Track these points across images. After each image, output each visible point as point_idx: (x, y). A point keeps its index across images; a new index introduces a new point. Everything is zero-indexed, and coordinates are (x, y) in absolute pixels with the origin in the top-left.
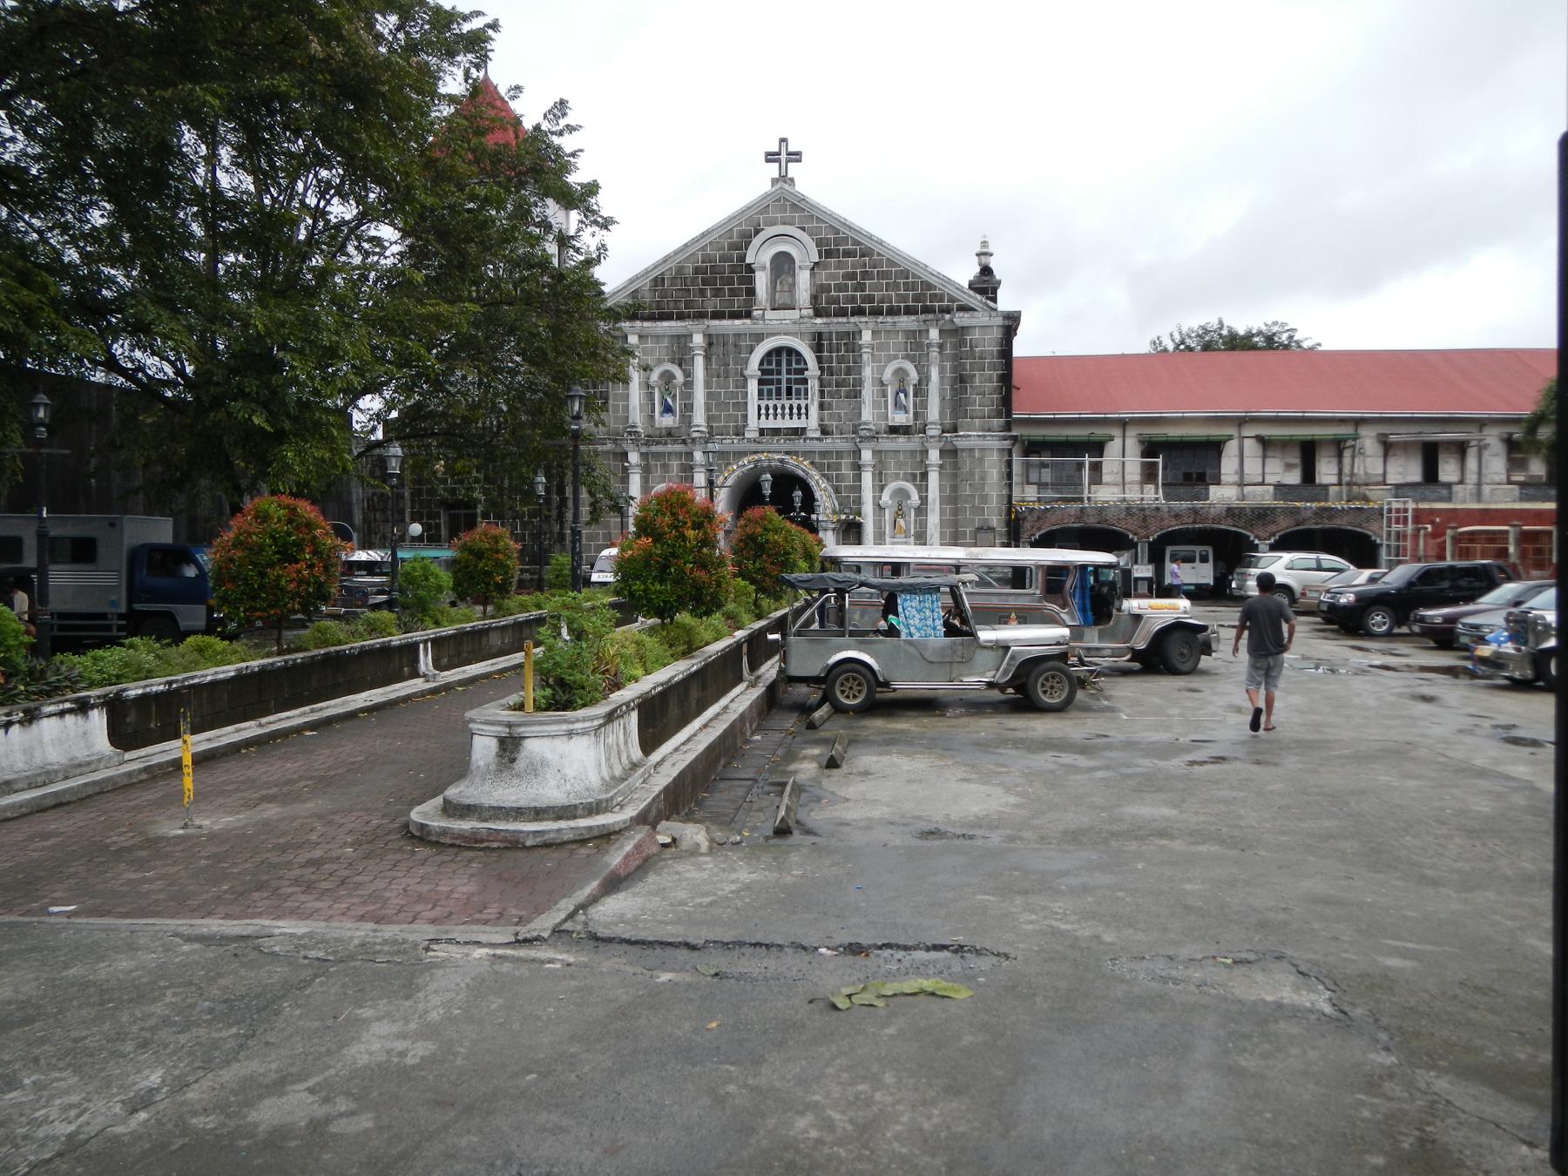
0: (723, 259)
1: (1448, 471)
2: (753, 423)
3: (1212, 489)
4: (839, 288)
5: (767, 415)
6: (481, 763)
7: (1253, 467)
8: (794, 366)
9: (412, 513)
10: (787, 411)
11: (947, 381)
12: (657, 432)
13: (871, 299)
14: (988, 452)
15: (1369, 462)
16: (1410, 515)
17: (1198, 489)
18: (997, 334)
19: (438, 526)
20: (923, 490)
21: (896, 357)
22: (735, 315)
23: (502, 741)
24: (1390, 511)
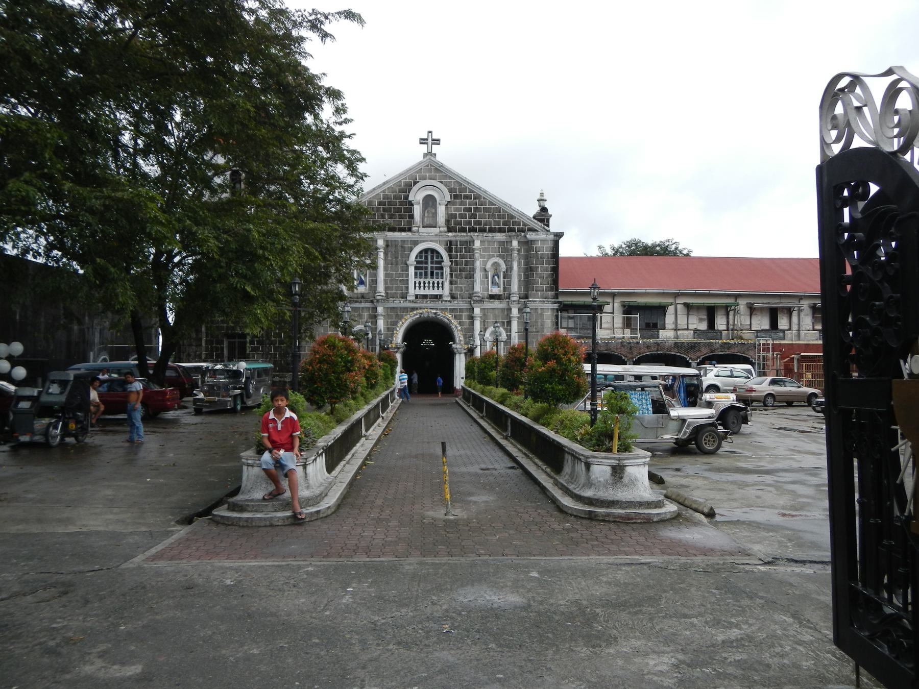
0: (395, 197)
1: (783, 323)
2: (412, 291)
3: (661, 332)
4: (461, 216)
5: (420, 287)
6: (602, 479)
7: (682, 321)
8: (435, 259)
9: (206, 341)
10: (431, 285)
11: (522, 270)
12: (356, 296)
13: (479, 223)
14: (545, 310)
15: (742, 319)
16: (771, 347)
17: (653, 332)
18: (550, 244)
19: (222, 349)
20: (509, 331)
21: (493, 256)
22: (402, 230)
23: (614, 468)
24: (759, 345)
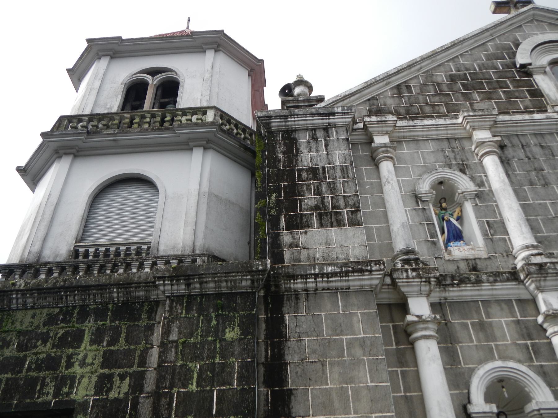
12: (451, 269)
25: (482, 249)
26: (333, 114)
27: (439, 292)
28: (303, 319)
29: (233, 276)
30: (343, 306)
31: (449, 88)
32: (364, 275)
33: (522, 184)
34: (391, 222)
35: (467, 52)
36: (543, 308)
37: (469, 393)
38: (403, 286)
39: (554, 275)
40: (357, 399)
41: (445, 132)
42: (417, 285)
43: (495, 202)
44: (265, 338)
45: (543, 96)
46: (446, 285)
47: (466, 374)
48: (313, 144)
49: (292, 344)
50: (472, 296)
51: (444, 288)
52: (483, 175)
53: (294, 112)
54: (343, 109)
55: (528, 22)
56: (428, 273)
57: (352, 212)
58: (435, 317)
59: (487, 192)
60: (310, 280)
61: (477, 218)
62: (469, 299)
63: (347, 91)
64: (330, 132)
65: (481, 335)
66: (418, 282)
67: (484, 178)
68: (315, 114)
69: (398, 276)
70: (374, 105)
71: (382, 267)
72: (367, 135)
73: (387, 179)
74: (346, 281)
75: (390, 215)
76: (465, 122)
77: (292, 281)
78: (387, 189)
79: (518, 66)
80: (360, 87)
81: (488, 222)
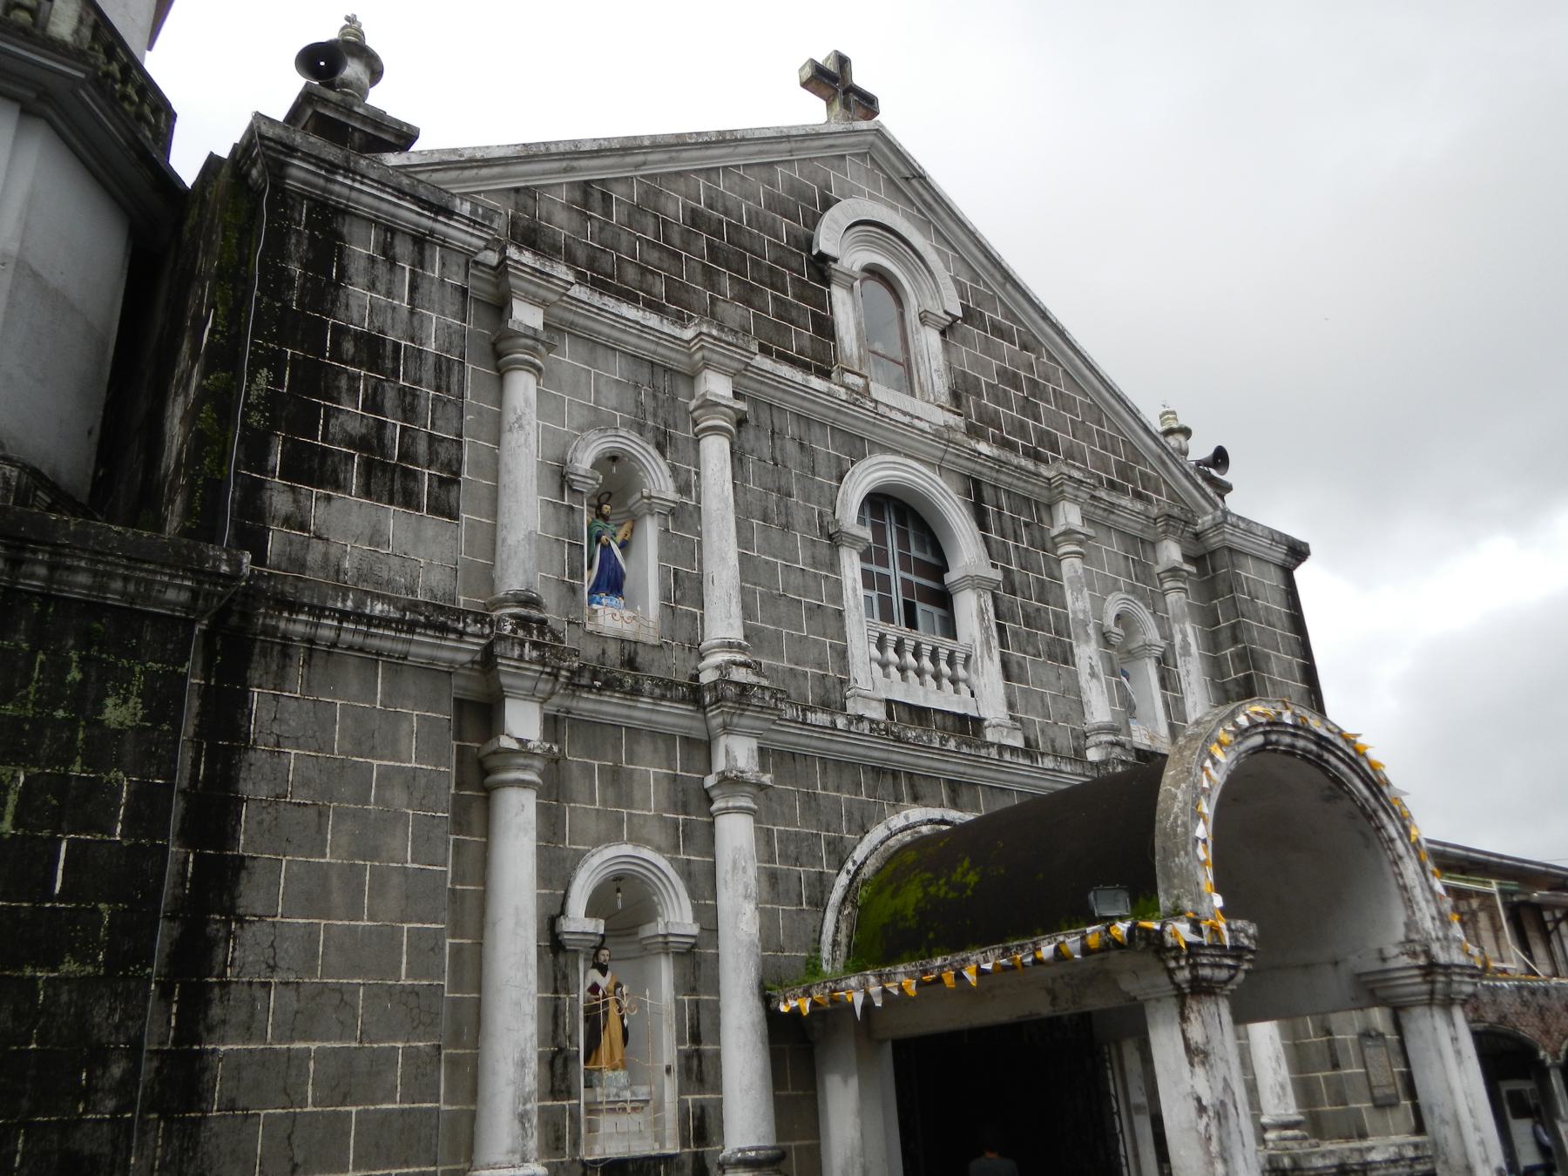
25: (651, 624)
26: (449, 213)
27: (562, 695)
28: (293, 705)
29: (147, 571)
30: (384, 693)
31: (683, 242)
32: (446, 639)
33: (751, 513)
34: (503, 519)
35: (737, 167)
36: (720, 764)
37: (565, 897)
38: (507, 672)
39: (758, 709)
40: (379, 887)
41: (652, 347)
42: (532, 678)
43: (700, 534)
44: (196, 734)
45: (834, 340)
46: (579, 686)
47: (568, 862)
48: (381, 270)
49: (258, 757)
50: (615, 715)
51: (574, 691)
52: (693, 469)
53: (357, 163)
54: (474, 212)
55: (857, 155)
56: (560, 659)
57: (441, 480)
58: (551, 748)
59: (691, 508)
60: (329, 622)
61: (660, 559)
62: (607, 719)
63: (480, 148)
64: (427, 253)
65: (610, 792)
66: (535, 671)
67: (694, 477)
68: (405, 194)
69: (503, 651)
70: (525, 209)
71: (487, 631)
72: (497, 286)
73: (519, 418)
74: (405, 641)
75: (505, 503)
76: (696, 344)
77: (286, 614)
78: (512, 439)
79: (815, 252)
80: (509, 153)
81: (676, 572)
